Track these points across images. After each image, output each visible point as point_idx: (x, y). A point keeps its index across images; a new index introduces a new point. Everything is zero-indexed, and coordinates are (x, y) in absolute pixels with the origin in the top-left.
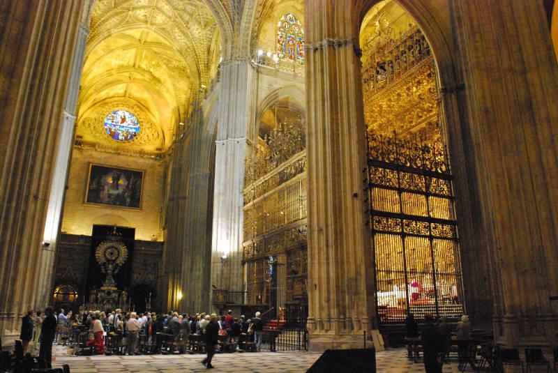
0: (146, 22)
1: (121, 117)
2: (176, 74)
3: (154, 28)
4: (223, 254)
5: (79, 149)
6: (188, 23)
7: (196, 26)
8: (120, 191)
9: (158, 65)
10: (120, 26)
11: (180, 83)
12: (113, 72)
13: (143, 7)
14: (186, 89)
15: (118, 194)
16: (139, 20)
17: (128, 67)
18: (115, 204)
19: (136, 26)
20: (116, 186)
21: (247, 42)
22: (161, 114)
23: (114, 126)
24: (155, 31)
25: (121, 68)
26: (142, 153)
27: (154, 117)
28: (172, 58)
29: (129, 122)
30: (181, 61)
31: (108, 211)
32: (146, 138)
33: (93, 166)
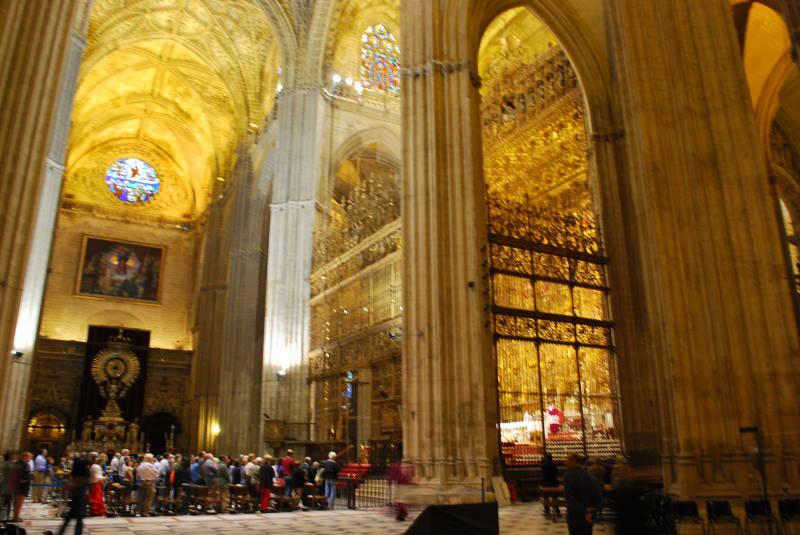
0: (170, 30)
2: (213, 106)
3: (181, 39)
4: (280, 368)
5: (68, 214)
6: (231, 33)
7: (244, 38)
8: (129, 276)
9: (186, 94)
13: (167, 9)
14: (228, 128)
15: (126, 282)
16: (160, 27)
17: (143, 95)
18: (120, 294)
20: (123, 269)
21: (317, 63)
22: (190, 164)
23: (122, 180)
24: (184, 45)
25: (133, 97)
26: (162, 221)
27: (179, 167)
28: (206, 83)
29: (145, 176)
31: (111, 306)
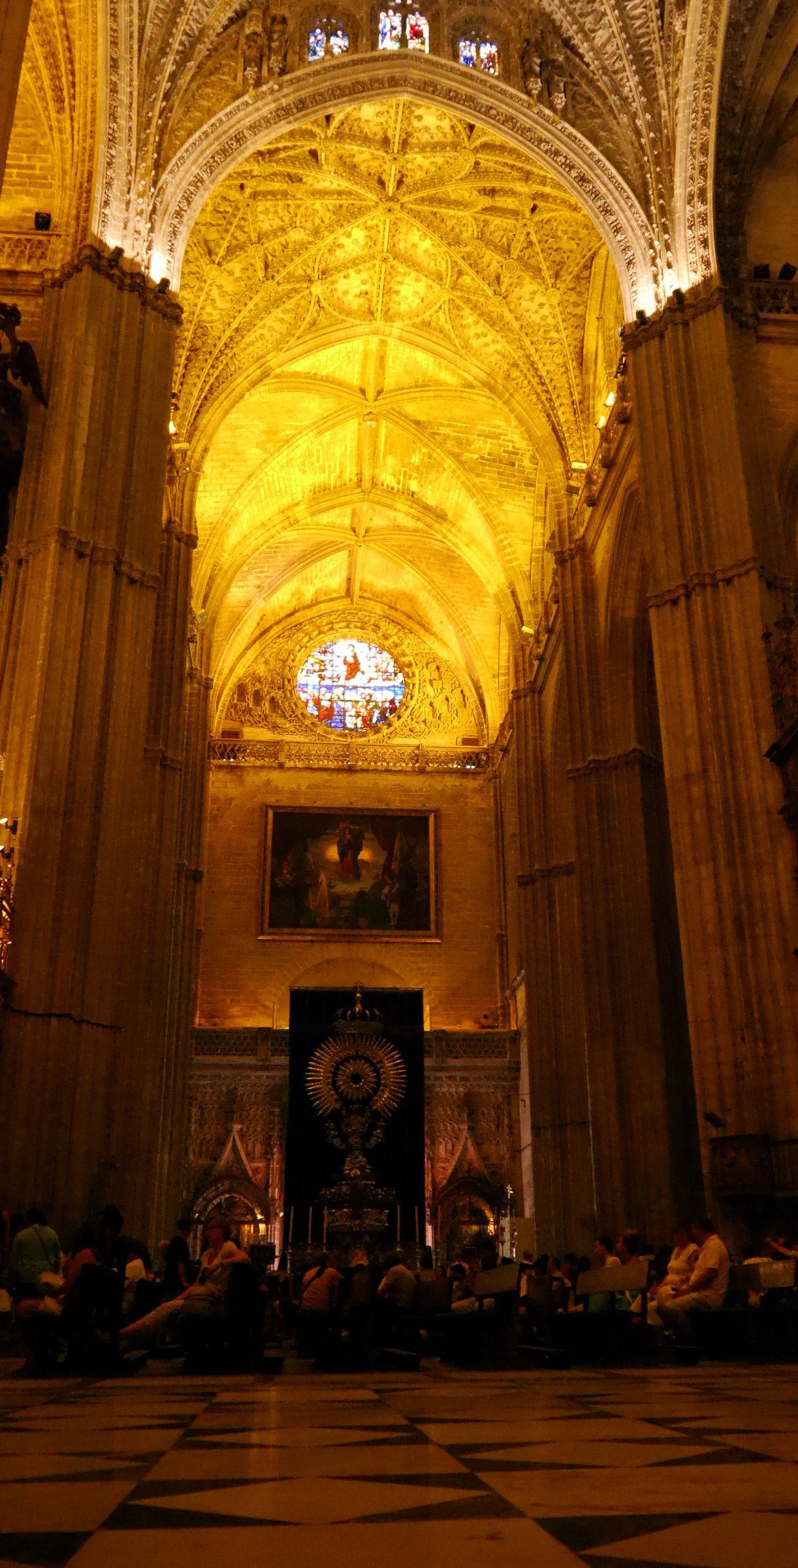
1: (345, 662)
2: (488, 480)
3: (396, 328)
5: (231, 769)
6: (498, 278)
7: (529, 285)
8: (366, 883)
9: (429, 466)
10: (293, 341)
11: (507, 507)
12: (301, 512)
13: (355, 263)
14: (528, 521)
15: (361, 893)
16: (349, 313)
17: (341, 488)
18: (355, 925)
19: (342, 334)
20: (350, 867)
22: (461, 629)
24: (401, 339)
25: (322, 497)
27: (445, 644)
30: (497, 436)
31: (336, 951)
32: (426, 709)
33: (274, 814)
